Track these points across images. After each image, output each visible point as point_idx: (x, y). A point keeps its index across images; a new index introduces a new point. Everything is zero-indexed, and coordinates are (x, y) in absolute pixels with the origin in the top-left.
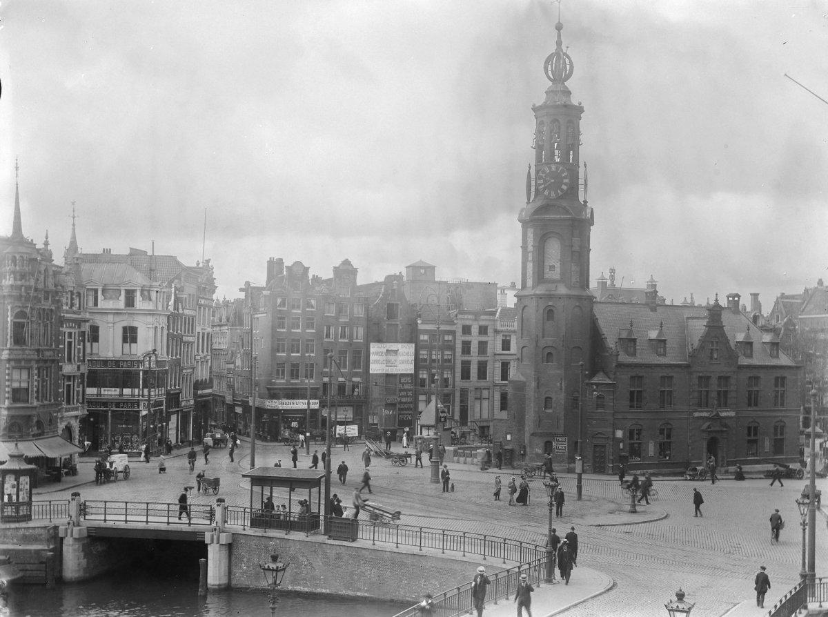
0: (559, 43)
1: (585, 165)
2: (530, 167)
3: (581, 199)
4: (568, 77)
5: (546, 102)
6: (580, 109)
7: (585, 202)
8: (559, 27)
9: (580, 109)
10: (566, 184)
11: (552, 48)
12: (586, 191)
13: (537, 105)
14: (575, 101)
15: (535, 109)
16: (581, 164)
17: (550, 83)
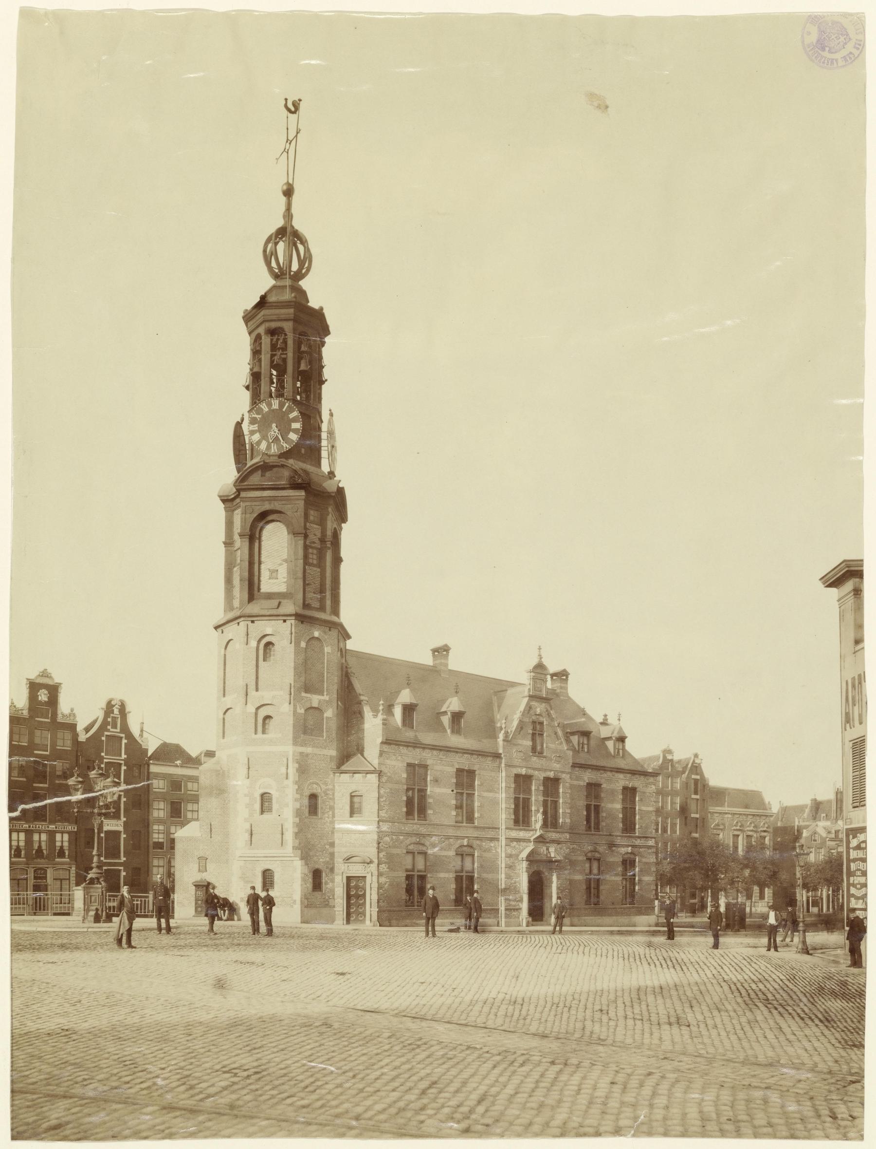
0: (288, 214)
1: (331, 415)
8: (288, 192)
12: (331, 455)
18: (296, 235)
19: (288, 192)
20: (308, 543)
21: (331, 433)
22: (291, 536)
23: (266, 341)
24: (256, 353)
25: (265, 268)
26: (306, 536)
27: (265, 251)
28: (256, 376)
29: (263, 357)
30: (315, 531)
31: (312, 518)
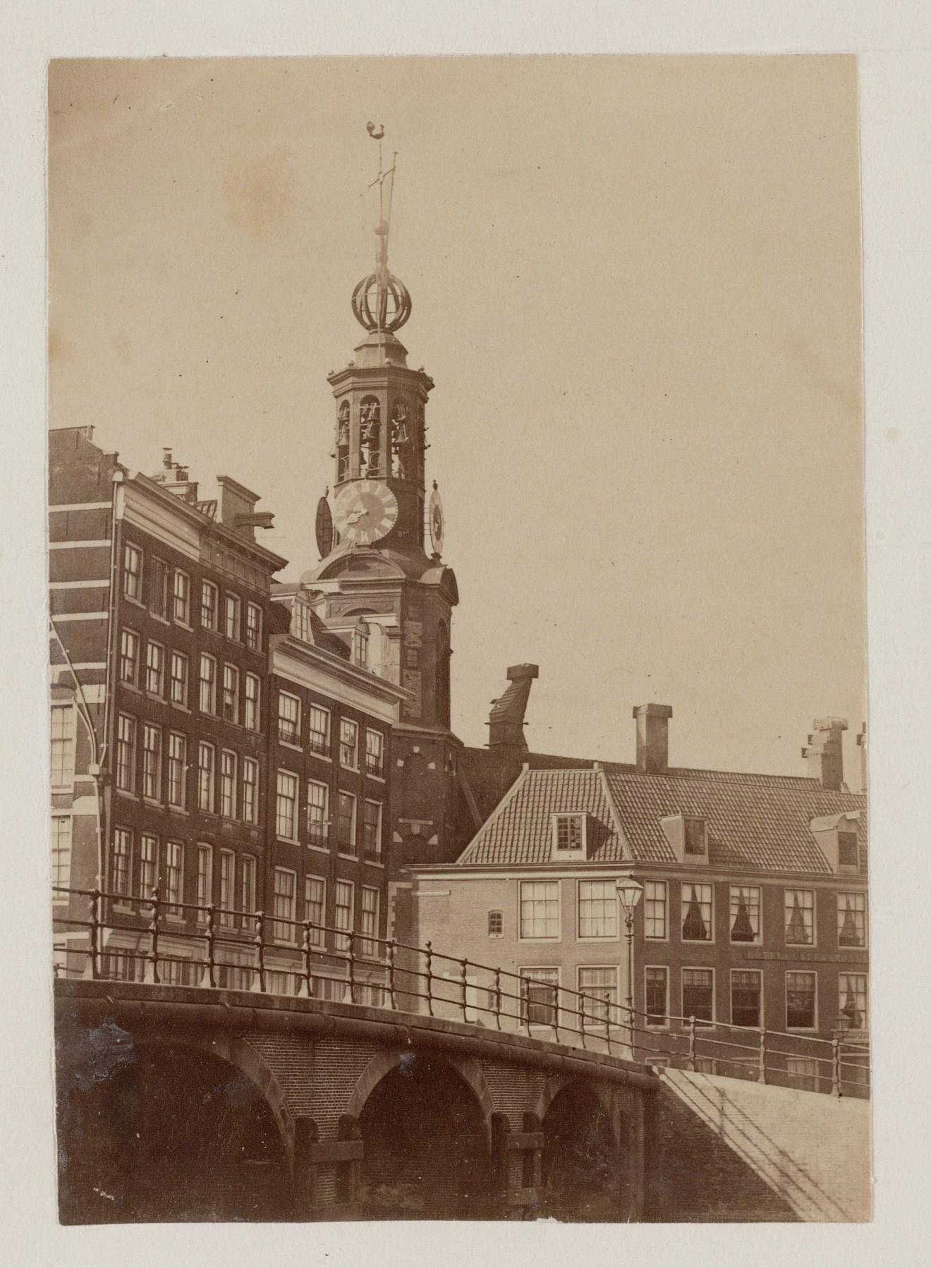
0: (383, 258)
1: (435, 486)
2: (327, 493)
3: (429, 551)
4: (397, 325)
5: (351, 365)
6: (423, 382)
7: (437, 556)
9: (423, 382)
10: (388, 517)
11: (371, 268)
12: (439, 534)
13: (337, 371)
14: (412, 364)
15: (334, 380)
16: (428, 486)
17: (367, 332)
18: (391, 281)
19: (383, 231)
20: (406, 644)
21: (437, 513)
22: (385, 636)
23: (355, 409)
24: (343, 423)
25: (357, 323)
26: (403, 638)
27: (354, 302)
28: (344, 451)
29: (351, 427)
30: (415, 628)
31: (411, 615)
